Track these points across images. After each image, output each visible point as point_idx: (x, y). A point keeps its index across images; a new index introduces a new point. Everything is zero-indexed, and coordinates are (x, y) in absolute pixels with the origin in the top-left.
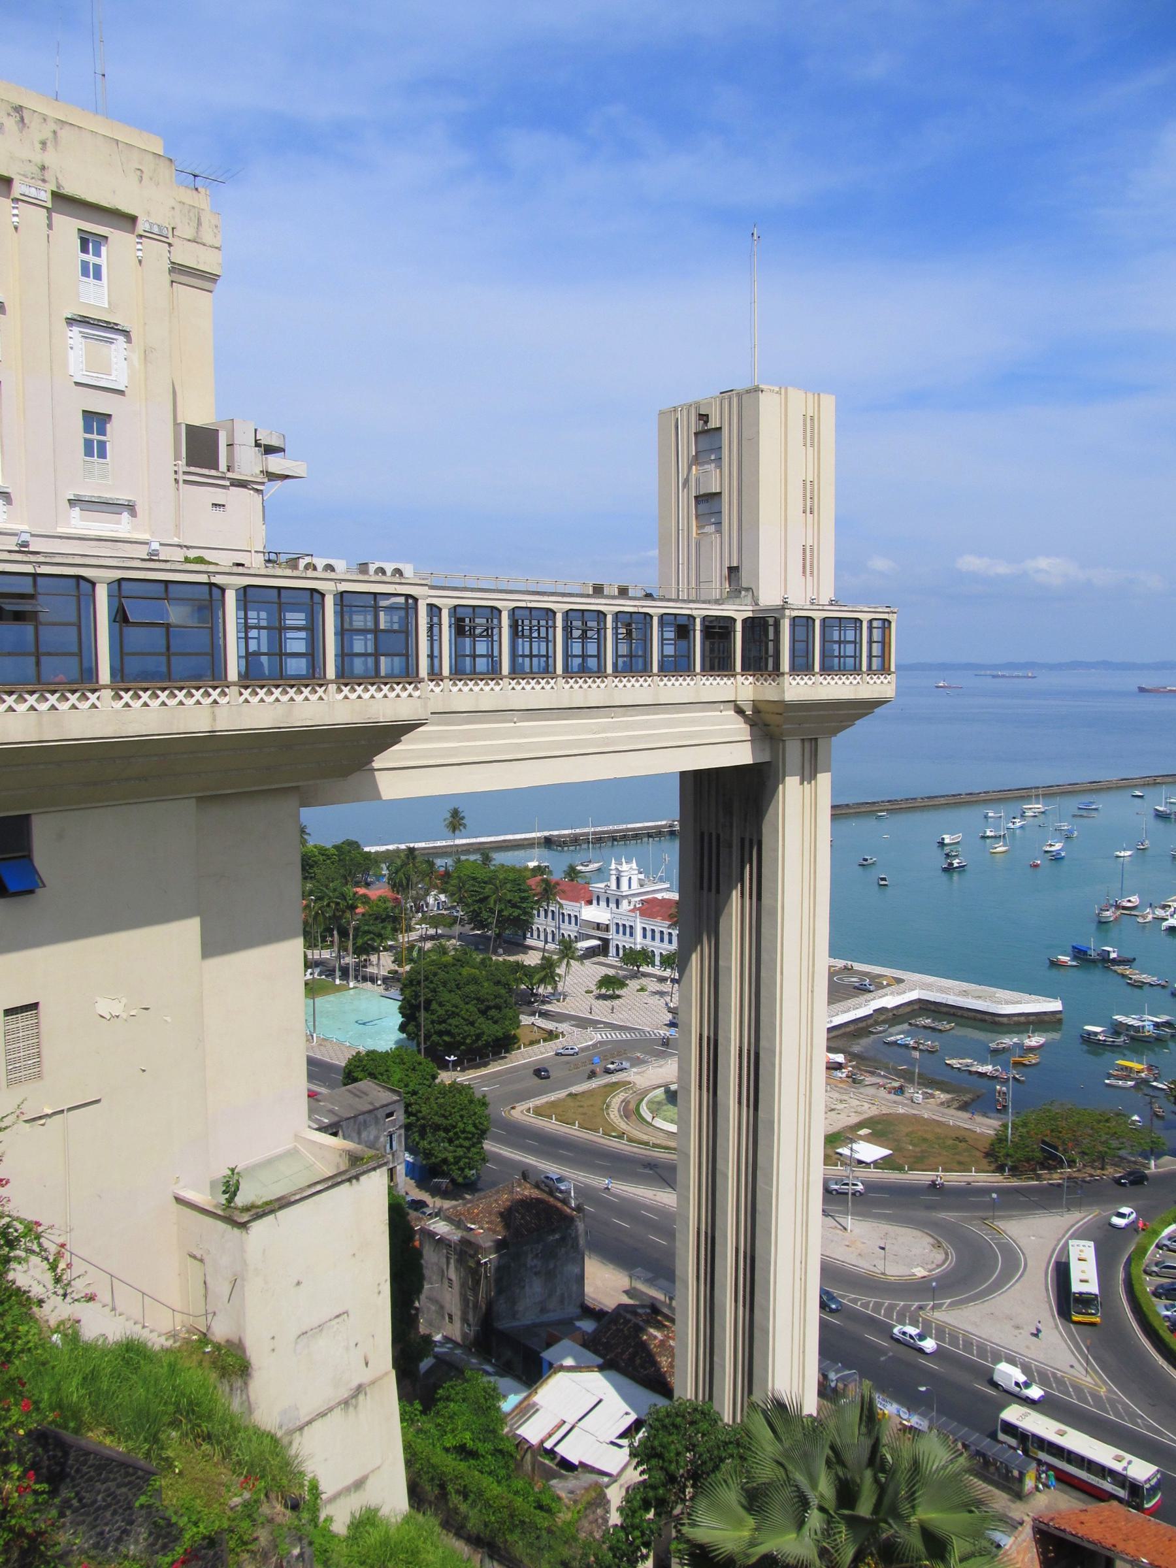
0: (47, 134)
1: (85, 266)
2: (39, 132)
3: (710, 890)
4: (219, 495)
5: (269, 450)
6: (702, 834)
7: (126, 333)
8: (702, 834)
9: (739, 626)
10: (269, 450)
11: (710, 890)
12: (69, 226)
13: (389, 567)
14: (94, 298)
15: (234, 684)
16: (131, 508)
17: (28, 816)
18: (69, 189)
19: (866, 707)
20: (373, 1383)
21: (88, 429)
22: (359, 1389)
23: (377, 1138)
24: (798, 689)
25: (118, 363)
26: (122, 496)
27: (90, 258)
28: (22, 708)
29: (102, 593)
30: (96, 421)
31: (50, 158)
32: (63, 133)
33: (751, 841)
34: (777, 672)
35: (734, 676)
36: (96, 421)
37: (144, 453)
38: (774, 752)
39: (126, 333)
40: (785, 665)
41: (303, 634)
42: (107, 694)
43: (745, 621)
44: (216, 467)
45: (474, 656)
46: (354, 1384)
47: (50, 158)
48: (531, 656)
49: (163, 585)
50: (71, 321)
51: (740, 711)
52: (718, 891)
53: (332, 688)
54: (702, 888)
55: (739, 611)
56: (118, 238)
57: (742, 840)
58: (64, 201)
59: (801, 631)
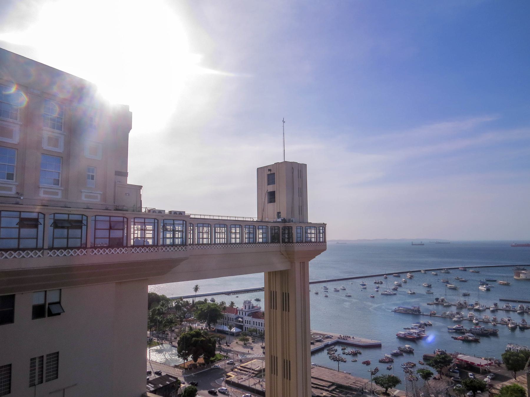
9: (281, 229)
35: (280, 243)
40: (295, 241)
41: (151, 232)
45: (203, 238)
48: (220, 238)
55: (281, 225)
59: (299, 231)
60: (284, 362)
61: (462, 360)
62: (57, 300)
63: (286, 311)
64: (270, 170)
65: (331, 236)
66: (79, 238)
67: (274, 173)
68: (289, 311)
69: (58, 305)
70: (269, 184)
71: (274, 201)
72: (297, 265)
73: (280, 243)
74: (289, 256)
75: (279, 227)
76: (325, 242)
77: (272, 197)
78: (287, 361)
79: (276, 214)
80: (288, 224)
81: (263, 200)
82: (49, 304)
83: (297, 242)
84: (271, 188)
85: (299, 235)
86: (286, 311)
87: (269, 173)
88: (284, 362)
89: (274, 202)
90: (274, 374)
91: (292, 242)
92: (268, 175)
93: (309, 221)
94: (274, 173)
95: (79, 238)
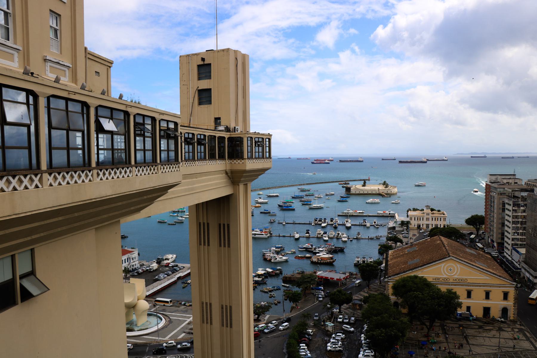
3: (204, 245)
6: (200, 224)
8: (200, 224)
9: (226, 140)
11: (204, 245)
15: (133, 166)
17: (34, 248)
19: (263, 171)
24: (250, 165)
33: (224, 225)
34: (242, 158)
38: (234, 190)
40: (246, 156)
43: (229, 138)
49: (109, 110)
51: (227, 173)
52: (209, 245)
54: (200, 244)
57: (220, 225)
59: (249, 142)
60: (222, 308)
61: (322, 277)
62: (29, 269)
63: (225, 246)
64: (203, 59)
65: (277, 151)
66: (80, 149)
67: (210, 64)
68: (229, 246)
69: (32, 277)
70: (199, 79)
71: (209, 102)
72: (241, 187)
73: (225, 160)
74: (235, 178)
75: (224, 138)
76: (270, 157)
77: (204, 97)
78: (226, 306)
79: (213, 120)
80: (234, 135)
81: (191, 101)
82: (22, 277)
83: (248, 158)
84: (204, 84)
85: (249, 148)
86: (225, 246)
87: (202, 63)
88: (222, 308)
89: (209, 102)
90: (207, 323)
91: (242, 158)
92: (199, 66)
93: (251, 131)
94: (210, 64)
95: (80, 149)
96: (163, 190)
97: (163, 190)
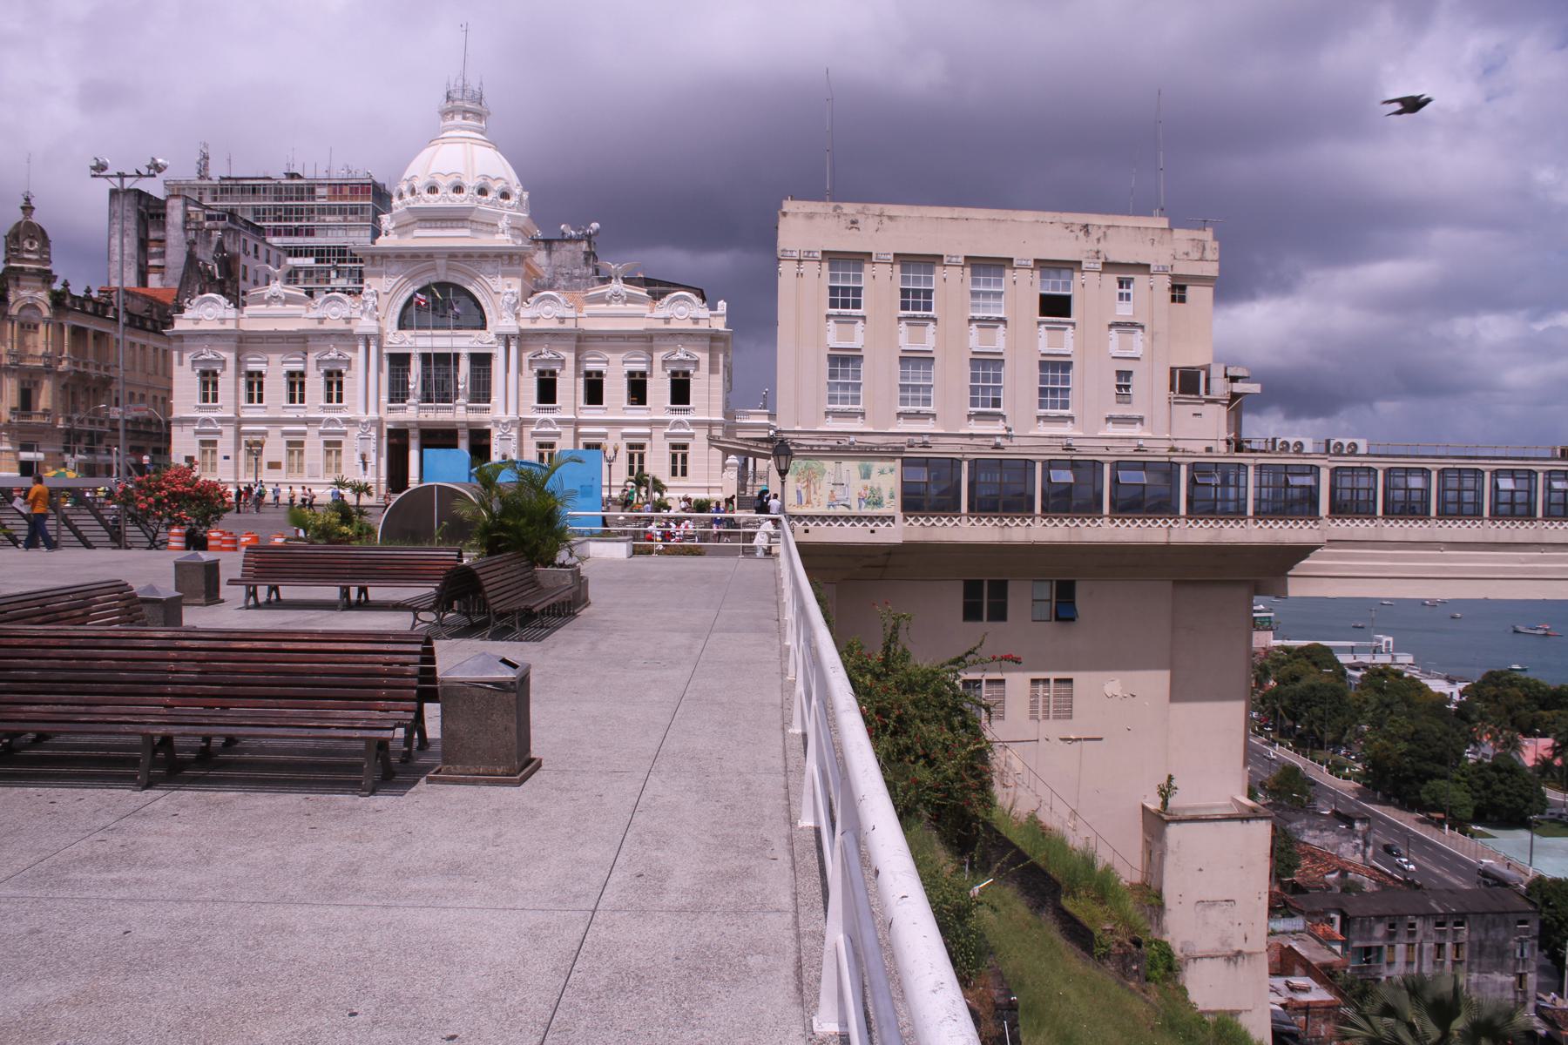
0: (1100, 234)
1: (1121, 295)
2: (1095, 234)
4: (1197, 409)
5: (1234, 379)
7: (1142, 327)
10: (1234, 379)
12: (1111, 279)
13: (1346, 442)
14: (1124, 311)
16: (1141, 419)
18: (1111, 259)
20: (1250, 954)
21: (1119, 379)
22: (1239, 953)
23: (1506, 940)
25: (1137, 344)
26: (1136, 414)
27: (1124, 291)
28: (1061, 526)
29: (1107, 468)
30: (1124, 375)
31: (1102, 246)
32: (1109, 232)
36: (1124, 375)
37: (1152, 388)
39: (1142, 327)
42: (1107, 520)
44: (1197, 392)
46: (1236, 948)
47: (1102, 246)
50: (1111, 326)
53: (1250, 521)
56: (1140, 280)
58: (1109, 266)
96: (1304, 551)
97: (1304, 551)
